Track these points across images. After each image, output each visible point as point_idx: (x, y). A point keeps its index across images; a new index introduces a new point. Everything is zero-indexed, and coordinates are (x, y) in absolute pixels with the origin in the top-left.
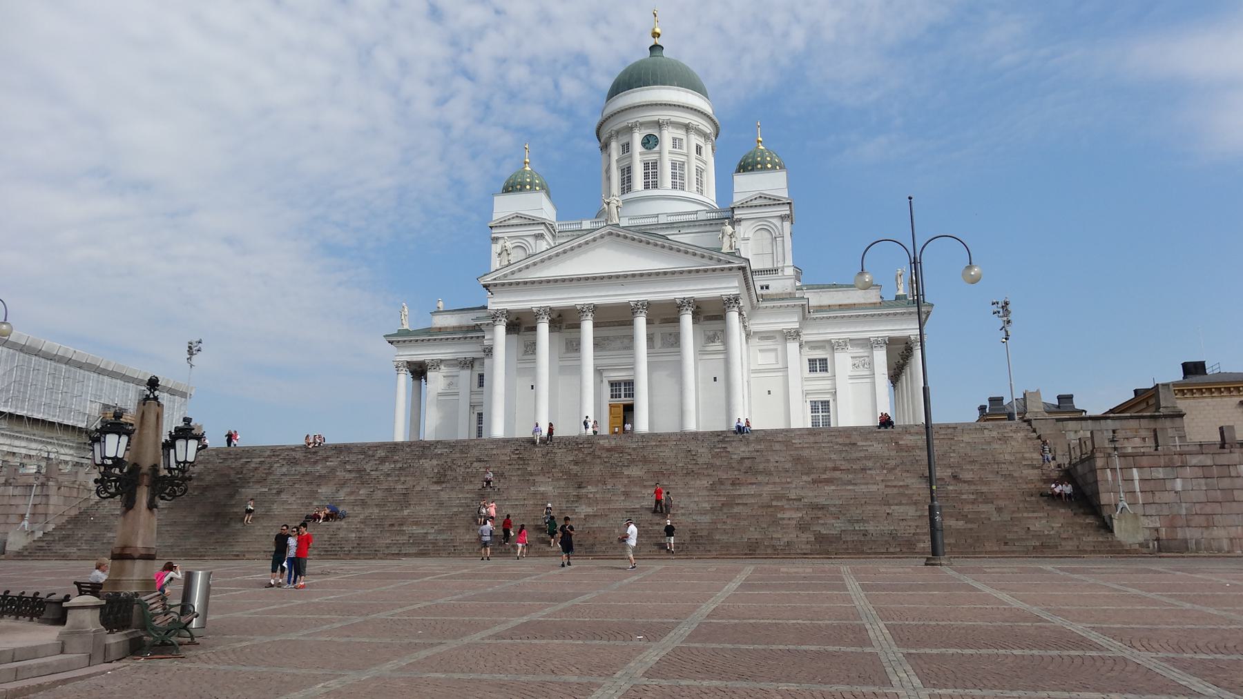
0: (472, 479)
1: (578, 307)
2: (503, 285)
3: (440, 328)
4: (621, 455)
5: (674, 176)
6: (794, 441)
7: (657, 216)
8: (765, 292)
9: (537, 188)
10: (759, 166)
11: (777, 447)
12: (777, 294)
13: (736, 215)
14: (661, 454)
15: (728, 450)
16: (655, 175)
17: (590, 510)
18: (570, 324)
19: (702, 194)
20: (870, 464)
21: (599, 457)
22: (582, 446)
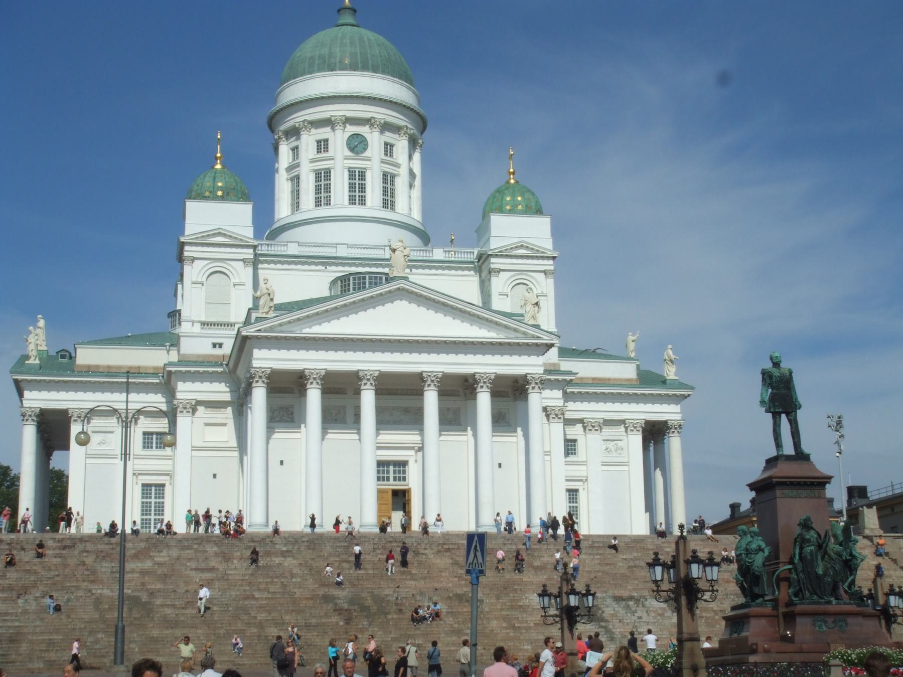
1: (361, 374)
3: (89, 367)
5: (385, 191)
10: (520, 207)
13: (493, 263)
16: (363, 188)
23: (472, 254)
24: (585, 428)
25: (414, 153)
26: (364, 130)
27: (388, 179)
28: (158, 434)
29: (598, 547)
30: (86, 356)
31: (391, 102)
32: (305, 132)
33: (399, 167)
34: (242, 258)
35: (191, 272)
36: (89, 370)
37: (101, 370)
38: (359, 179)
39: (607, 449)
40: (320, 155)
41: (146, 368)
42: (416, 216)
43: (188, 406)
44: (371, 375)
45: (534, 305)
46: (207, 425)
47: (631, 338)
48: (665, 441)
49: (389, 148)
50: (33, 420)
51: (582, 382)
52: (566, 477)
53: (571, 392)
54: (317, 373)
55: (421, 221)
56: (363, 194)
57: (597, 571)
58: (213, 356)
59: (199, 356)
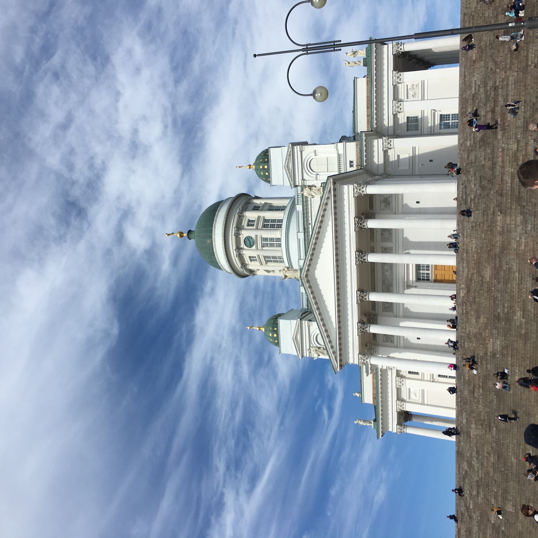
2: (340, 355)
3: (374, 398)
4: (473, 281)
5: (273, 226)
7: (299, 240)
8: (355, 164)
9: (276, 322)
11: (472, 157)
12: (357, 155)
14: (474, 250)
15: (473, 198)
16: (272, 239)
17: (519, 314)
18: (372, 308)
19: (286, 207)
20: (490, 84)
21: (474, 298)
22: (465, 311)
26: (242, 237)
30: (368, 398)
33: (260, 216)
34: (308, 327)
36: (375, 398)
37: (375, 392)
39: (413, 96)
44: (359, 295)
45: (311, 190)
49: (250, 223)
51: (370, 116)
53: (376, 125)
54: (360, 327)
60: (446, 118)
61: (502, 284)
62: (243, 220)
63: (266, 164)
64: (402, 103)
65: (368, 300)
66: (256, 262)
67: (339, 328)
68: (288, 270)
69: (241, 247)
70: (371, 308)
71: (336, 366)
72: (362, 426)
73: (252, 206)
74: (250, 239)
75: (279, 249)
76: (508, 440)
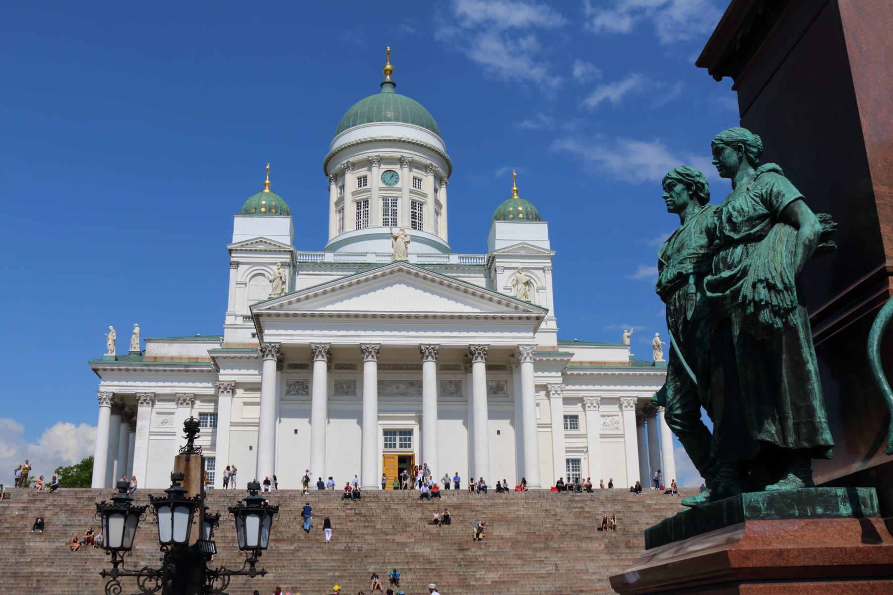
0: (318, 538)
1: (363, 347)
2: (278, 315)
3: (155, 358)
4: (474, 513)
5: (413, 215)
6: (648, 502)
10: (521, 216)
16: (395, 213)
23: (483, 259)
24: (584, 406)
25: (440, 188)
26: (396, 168)
27: (417, 207)
28: (211, 414)
29: (579, 500)
31: (417, 144)
32: (349, 171)
33: (426, 197)
35: (236, 275)
37: (165, 360)
38: (392, 206)
40: (361, 188)
41: (203, 358)
42: (443, 236)
43: (229, 388)
44: (373, 348)
46: (245, 404)
47: (626, 334)
48: (657, 417)
49: (417, 181)
50: (107, 403)
51: (581, 365)
52: (566, 448)
53: (571, 374)
54: (323, 347)
55: (446, 240)
56: (395, 217)
57: (574, 525)
58: (252, 344)
59: (240, 344)
60: (576, 467)
61: (514, 553)
62: (422, 170)
63: (525, 217)
64: (597, 409)
65: (365, 360)
66: (357, 185)
67: (322, 316)
68: (405, 243)
69: (382, 165)
70: (341, 363)
71: (262, 308)
72: (106, 339)
73: (438, 187)
74: (394, 178)
75: (381, 224)
76: (293, 568)
